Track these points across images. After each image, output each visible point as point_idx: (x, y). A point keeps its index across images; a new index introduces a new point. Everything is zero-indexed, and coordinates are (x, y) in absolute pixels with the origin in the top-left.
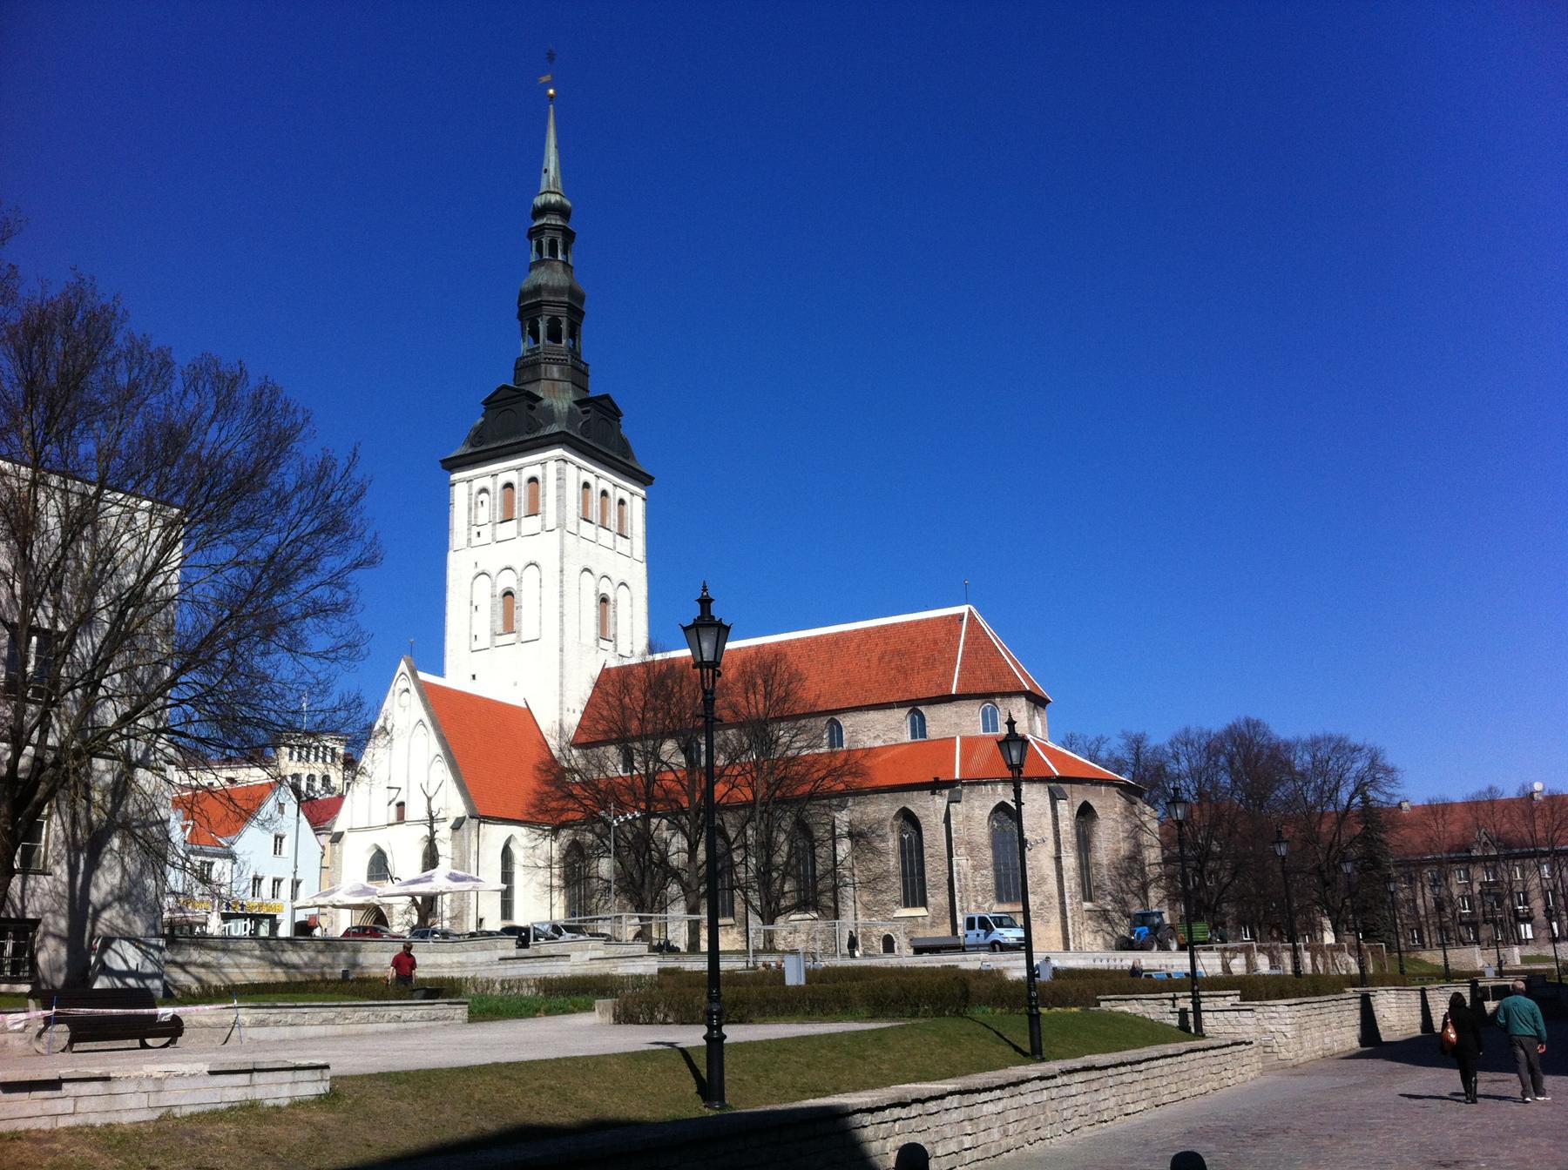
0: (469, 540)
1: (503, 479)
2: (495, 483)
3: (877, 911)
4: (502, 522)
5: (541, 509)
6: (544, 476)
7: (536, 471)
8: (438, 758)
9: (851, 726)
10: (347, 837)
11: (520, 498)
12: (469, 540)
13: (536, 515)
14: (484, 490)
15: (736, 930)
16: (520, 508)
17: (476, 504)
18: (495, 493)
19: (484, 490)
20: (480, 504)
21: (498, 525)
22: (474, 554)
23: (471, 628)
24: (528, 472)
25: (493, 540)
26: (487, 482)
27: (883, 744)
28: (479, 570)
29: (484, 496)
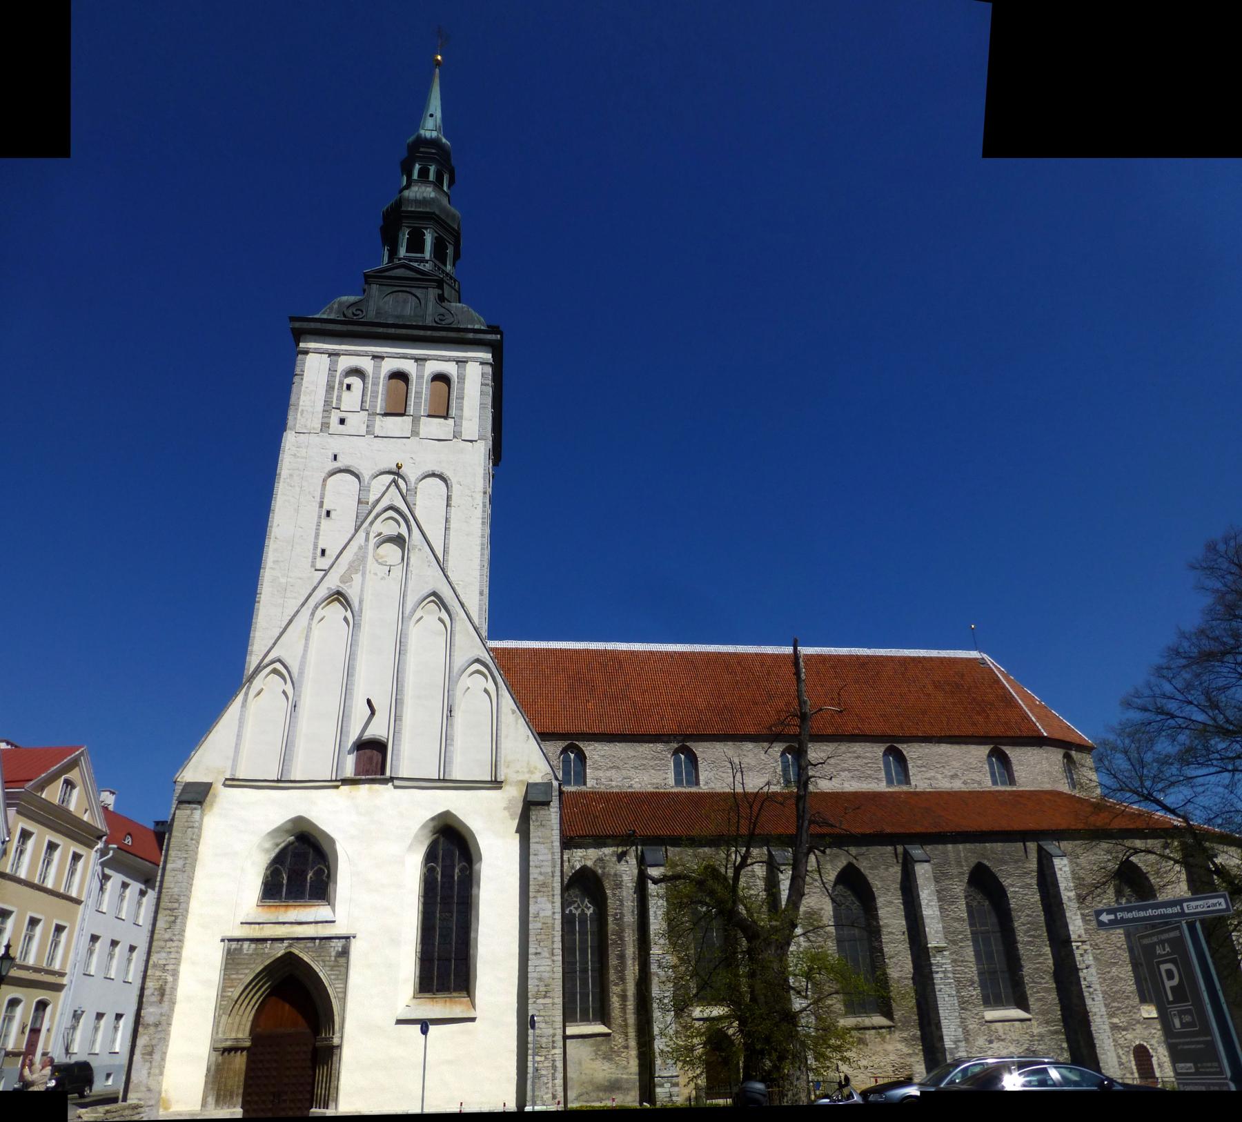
0: (325, 426)
1: (389, 365)
2: (377, 369)
3: (1119, 1008)
4: (386, 414)
5: (453, 412)
6: (462, 378)
7: (450, 369)
8: (477, 666)
9: (919, 758)
10: (225, 798)
11: (418, 394)
12: (325, 426)
13: (446, 417)
14: (357, 372)
15: (897, 1035)
16: (417, 404)
17: (341, 383)
18: (376, 378)
19: (357, 372)
20: (345, 386)
21: (378, 417)
22: (335, 445)
23: (317, 535)
24: (432, 367)
25: (368, 433)
26: (366, 364)
27: (964, 788)
28: (339, 464)
29: (355, 381)
